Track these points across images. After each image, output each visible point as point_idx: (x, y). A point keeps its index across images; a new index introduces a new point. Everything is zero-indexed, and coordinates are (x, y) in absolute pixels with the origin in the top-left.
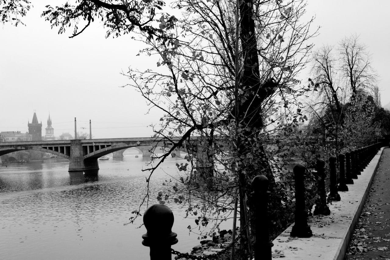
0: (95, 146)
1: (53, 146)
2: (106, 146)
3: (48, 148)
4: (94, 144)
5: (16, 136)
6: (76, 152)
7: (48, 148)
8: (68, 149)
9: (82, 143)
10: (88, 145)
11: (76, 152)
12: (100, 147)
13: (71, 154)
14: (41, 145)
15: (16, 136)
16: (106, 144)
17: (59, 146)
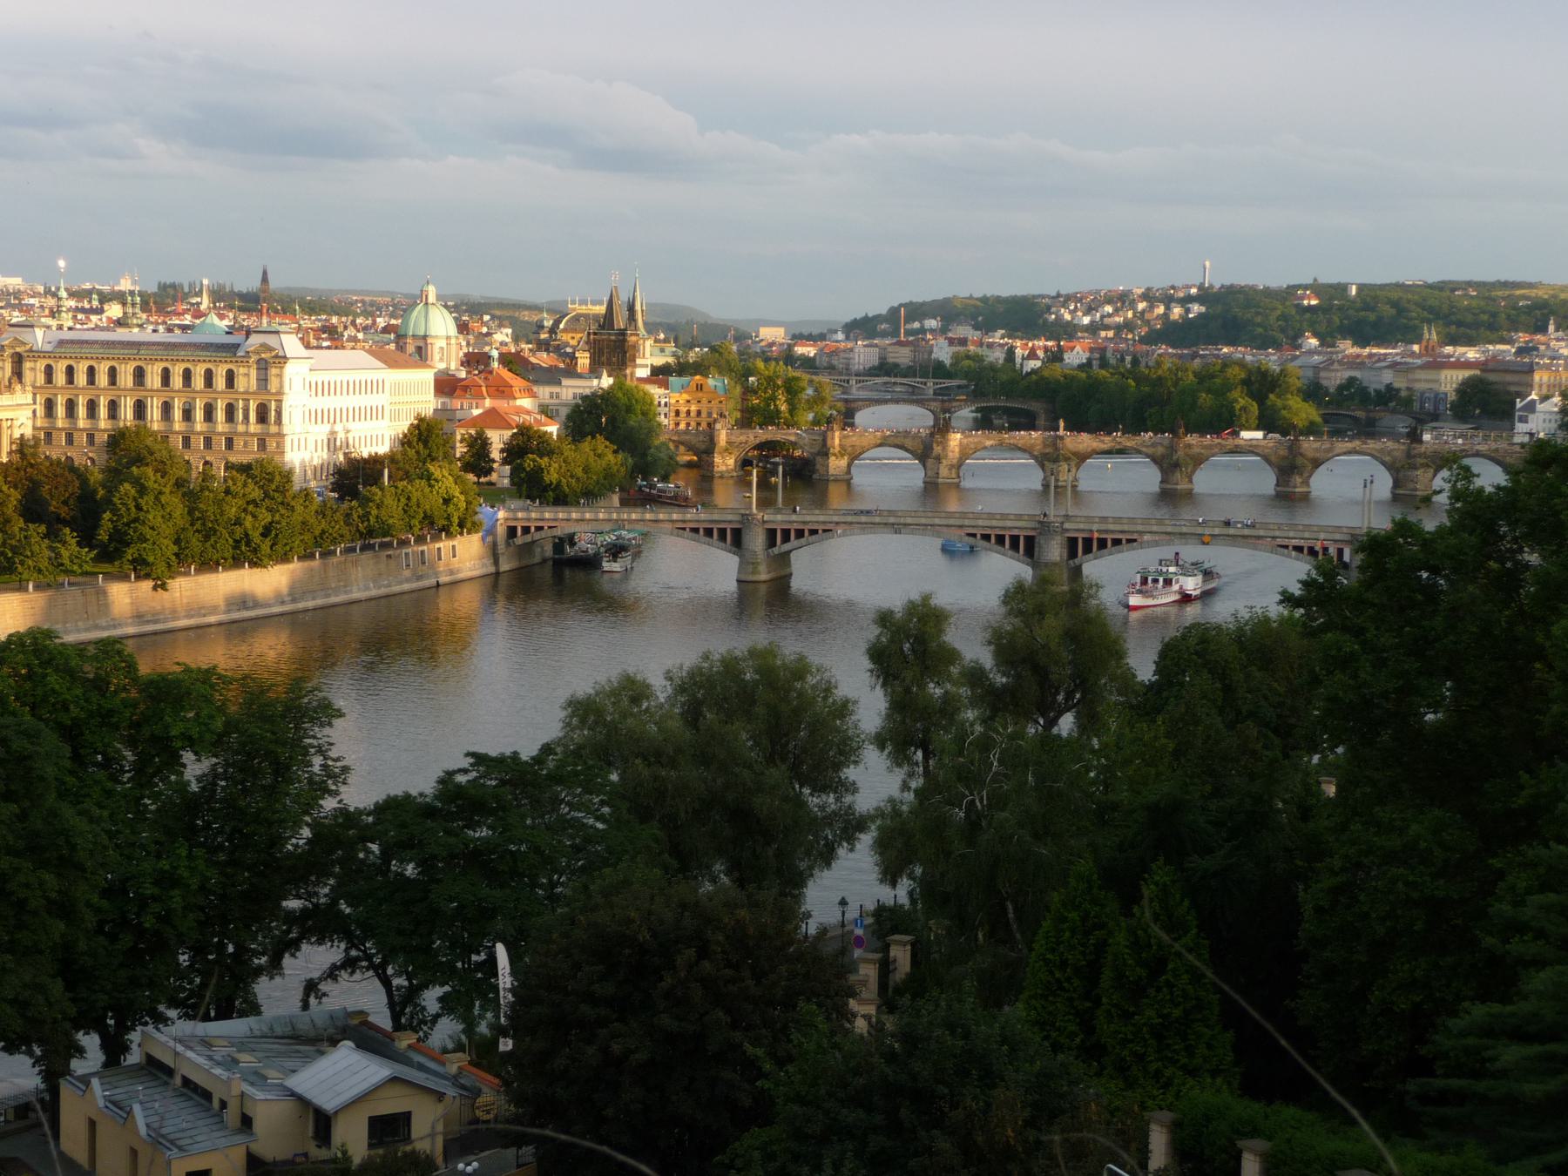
0: (1098, 539)
1: (993, 533)
2: (1124, 542)
3: (979, 536)
4: (1096, 535)
5: (567, 387)
6: (1054, 551)
7: (979, 536)
8: (1030, 541)
9: (1067, 530)
10: (1080, 536)
11: (1054, 551)
12: (1109, 543)
13: (1036, 554)
14: (961, 527)
15: (567, 387)
16: (1123, 537)
17: (1007, 533)
